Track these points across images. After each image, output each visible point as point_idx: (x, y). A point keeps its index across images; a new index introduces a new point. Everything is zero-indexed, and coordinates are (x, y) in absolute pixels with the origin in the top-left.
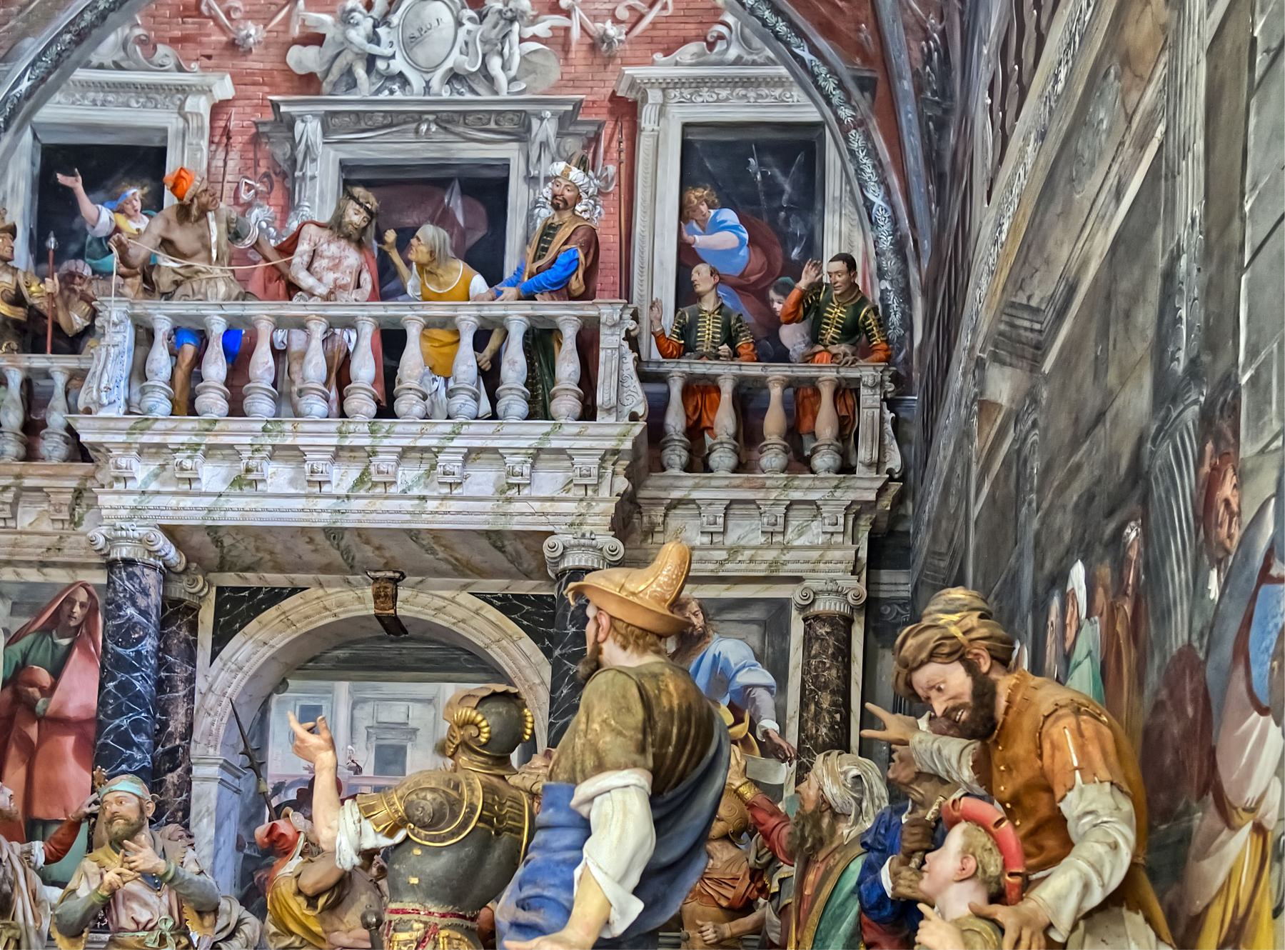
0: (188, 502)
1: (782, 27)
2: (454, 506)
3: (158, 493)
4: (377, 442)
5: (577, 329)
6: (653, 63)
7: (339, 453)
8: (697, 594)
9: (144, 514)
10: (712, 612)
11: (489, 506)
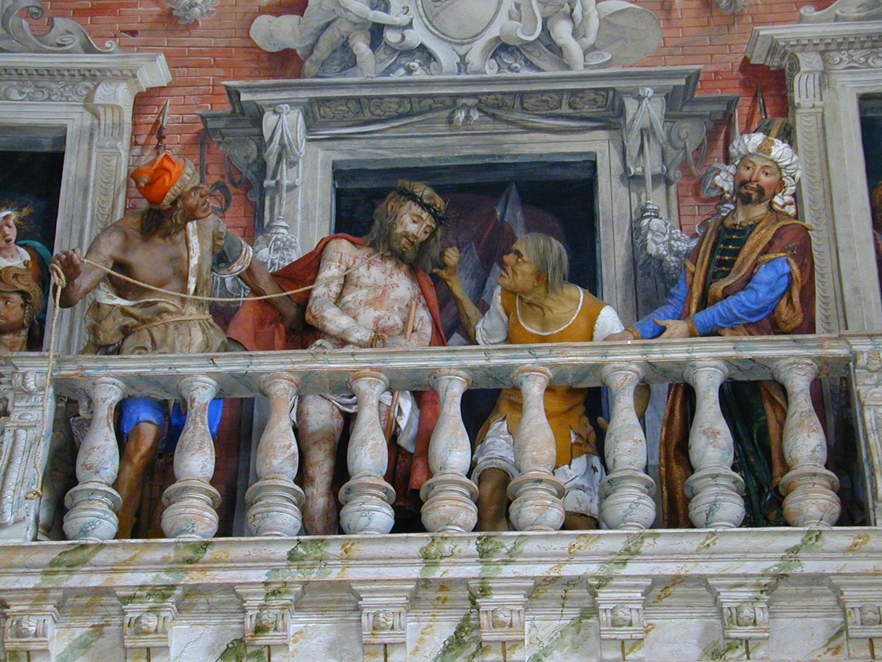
5: (812, 377)
6: (801, 20)
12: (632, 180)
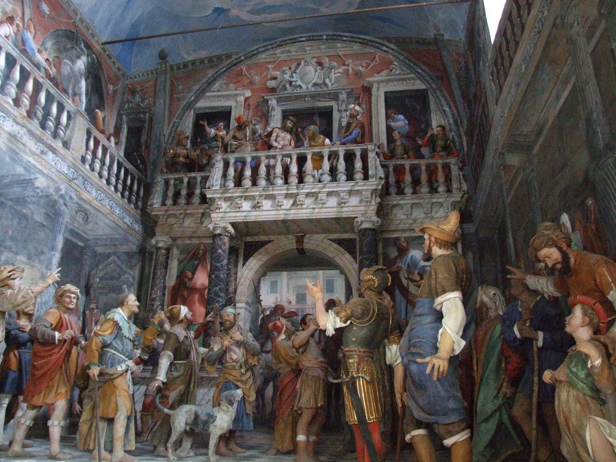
0: (239, 214)
1: (411, 64)
2: (324, 210)
3: (230, 212)
6: (374, 76)
7: (287, 196)
8: (404, 235)
11: (335, 210)
12: (340, 111)
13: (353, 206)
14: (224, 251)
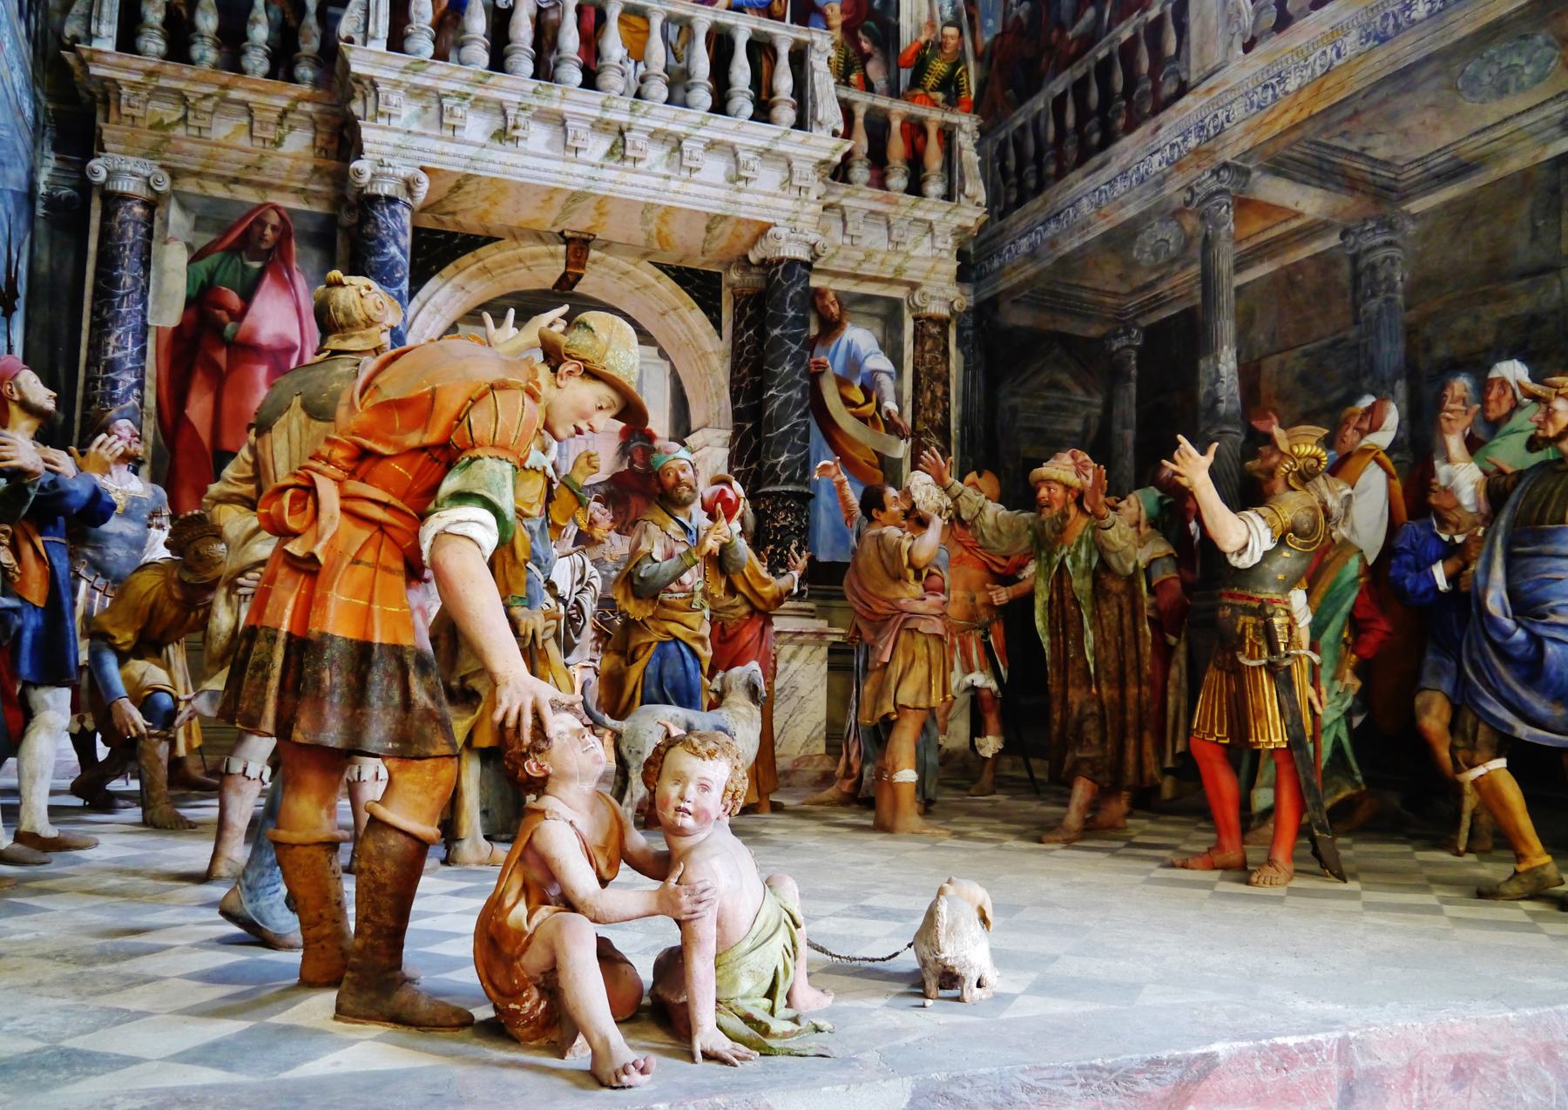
0: (452, 148)
2: (693, 188)
4: (633, 120)
7: (601, 126)
9: (408, 153)
10: (845, 303)
11: (722, 193)
13: (769, 194)
14: (403, 252)
